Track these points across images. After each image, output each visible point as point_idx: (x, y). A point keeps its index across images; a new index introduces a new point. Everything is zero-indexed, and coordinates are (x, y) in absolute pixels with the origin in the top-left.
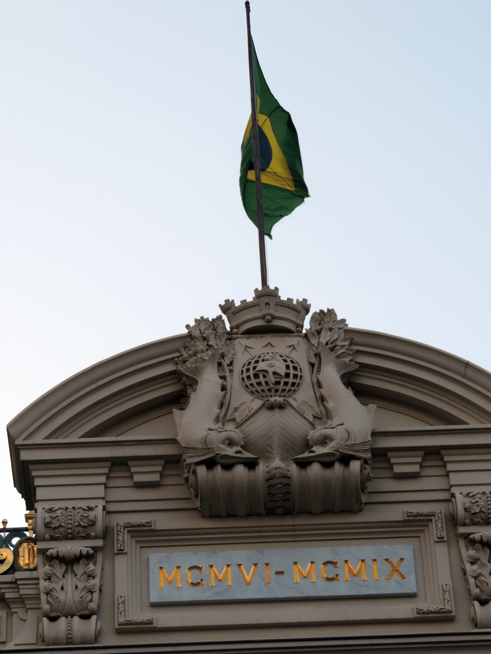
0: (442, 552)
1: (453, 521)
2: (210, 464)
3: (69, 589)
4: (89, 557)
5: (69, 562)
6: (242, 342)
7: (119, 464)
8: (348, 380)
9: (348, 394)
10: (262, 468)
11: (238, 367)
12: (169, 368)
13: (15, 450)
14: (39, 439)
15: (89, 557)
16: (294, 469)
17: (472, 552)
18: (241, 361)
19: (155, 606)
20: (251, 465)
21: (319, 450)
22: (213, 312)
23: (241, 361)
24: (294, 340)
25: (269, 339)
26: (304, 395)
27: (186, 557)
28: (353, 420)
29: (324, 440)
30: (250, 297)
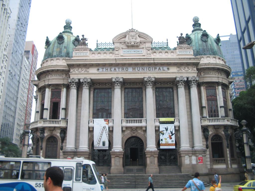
1: (146, 48)
3: (117, 52)
4: (118, 50)
5: (117, 50)
7: (121, 43)
8: (138, 36)
9: (138, 37)
10: (131, 43)
13: (113, 41)
15: (118, 50)
17: (147, 50)
19: (123, 54)
20: (131, 43)
21: (136, 42)
22: (128, 30)
24: (134, 32)
26: (135, 37)
28: (139, 40)
29: (136, 41)
30: (131, 29)
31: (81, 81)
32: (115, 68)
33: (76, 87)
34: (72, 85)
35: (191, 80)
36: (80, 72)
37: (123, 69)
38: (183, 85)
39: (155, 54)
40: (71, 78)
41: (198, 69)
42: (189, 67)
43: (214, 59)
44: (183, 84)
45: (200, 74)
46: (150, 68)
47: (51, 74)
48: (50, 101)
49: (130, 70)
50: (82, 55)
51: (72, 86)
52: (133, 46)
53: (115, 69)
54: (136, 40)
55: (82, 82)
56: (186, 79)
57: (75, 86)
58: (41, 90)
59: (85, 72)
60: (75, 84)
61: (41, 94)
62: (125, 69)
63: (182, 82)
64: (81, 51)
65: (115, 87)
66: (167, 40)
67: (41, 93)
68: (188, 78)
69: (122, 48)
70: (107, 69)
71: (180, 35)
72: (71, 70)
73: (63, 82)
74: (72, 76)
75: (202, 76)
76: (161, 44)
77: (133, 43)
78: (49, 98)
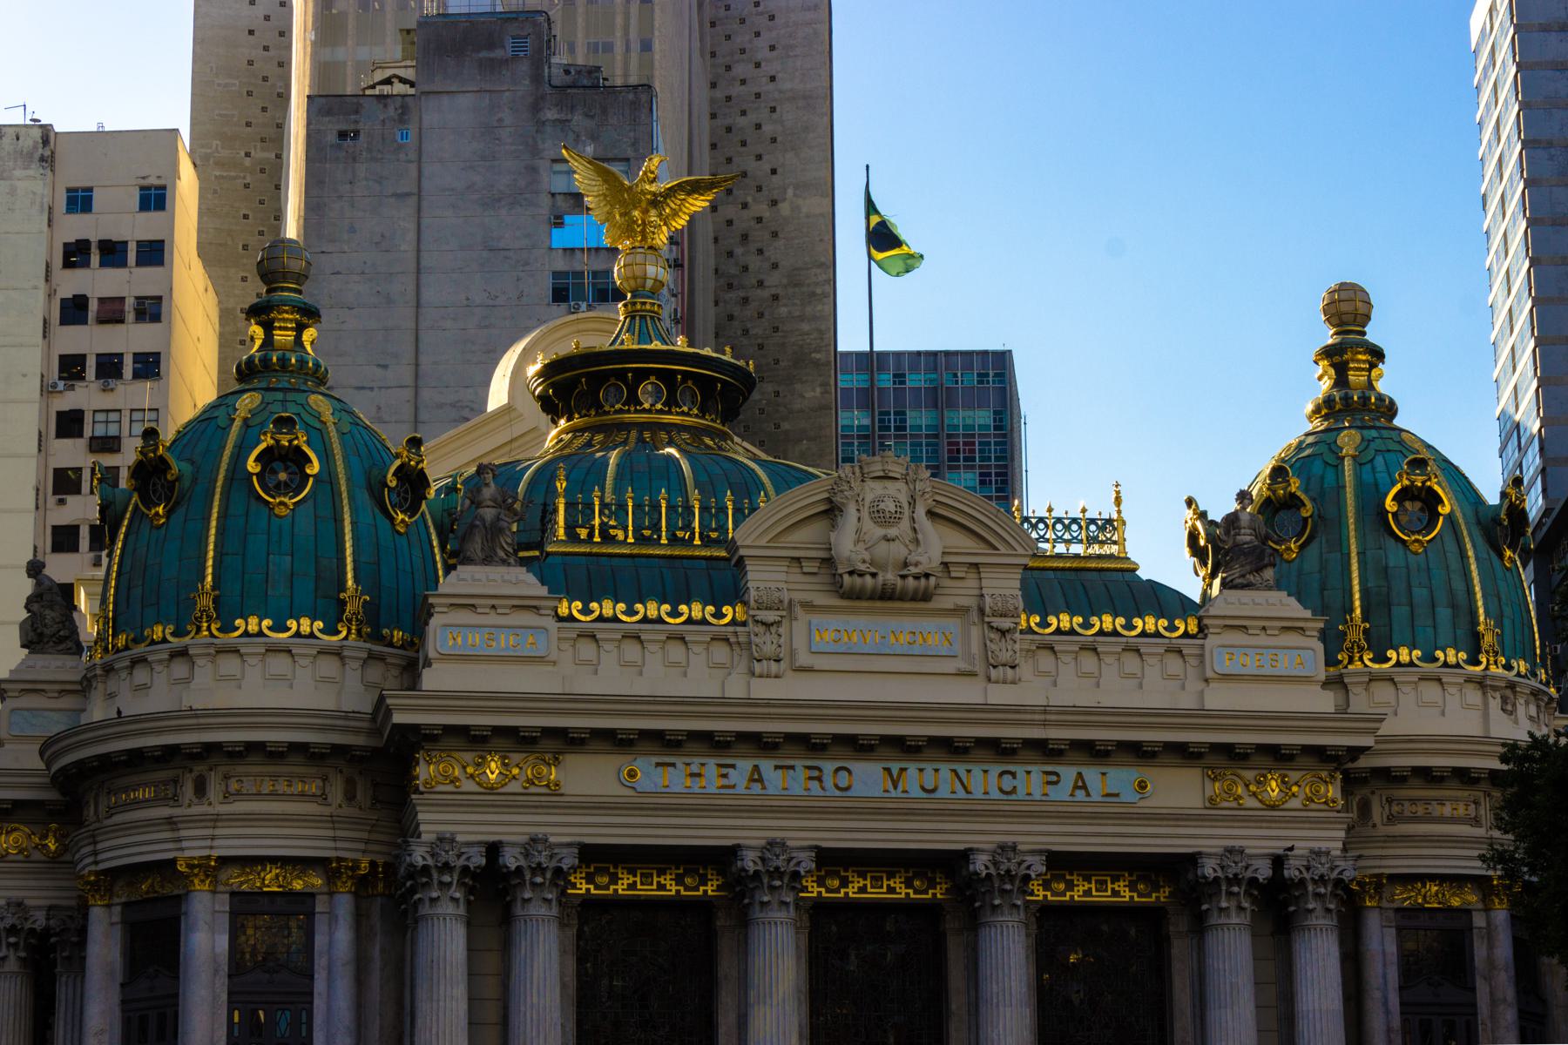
0: (975, 632)
1: (982, 611)
2: (851, 573)
4: (778, 623)
6: (870, 484)
7: (798, 559)
8: (931, 514)
10: (880, 578)
11: (867, 504)
12: (826, 495)
14: (748, 542)
15: (778, 623)
16: (899, 582)
18: (869, 497)
20: (874, 575)
21: (913, 570)
23: (869, 497)
24: (901, 485)
25: (888, 484)
27: (834, 621)
31: (511, 860)
32: (756, 768)
33: (469, 903)
34: (435, 895)
35: (1306, 875)
36: (491, 789)
37: (816, 773)
38: (1241, 908)
39: (1046, 660)
40: (428, 831)
41: (1351, 782)
42: (1294, 776)
43: (1474, 696)
44: (1246, 905)
45: (1365, 809)
46: (1014, 775)
47: (226, 777)
48: (225, 997)
49: (868, 777)
50: (505, 642)
51: (433, 901)
52: (886, 595)
53: (756, 777)
54: (913, 558)
55: (513, 867)
56: (1264, 872)
57: (455, 900)
58: (110, 892)
59: (533, 790)
60: (461, 884)
61: (123, 922)
62: (829, 781)
63: (1236, 889)
64: (493, 619)
65: (757, 913)
66: (1118, 501)
67: (116, 918)
68: (1278, 861)
69: (809, 606)
70: (694, 769)
71: (1233, 506)
72: (425, 771)
73: (331, 844)
74: (431, 822)
75: (1383, 830)
76: (1067, 528)
77: (890, 577)
78: (216, 972)
